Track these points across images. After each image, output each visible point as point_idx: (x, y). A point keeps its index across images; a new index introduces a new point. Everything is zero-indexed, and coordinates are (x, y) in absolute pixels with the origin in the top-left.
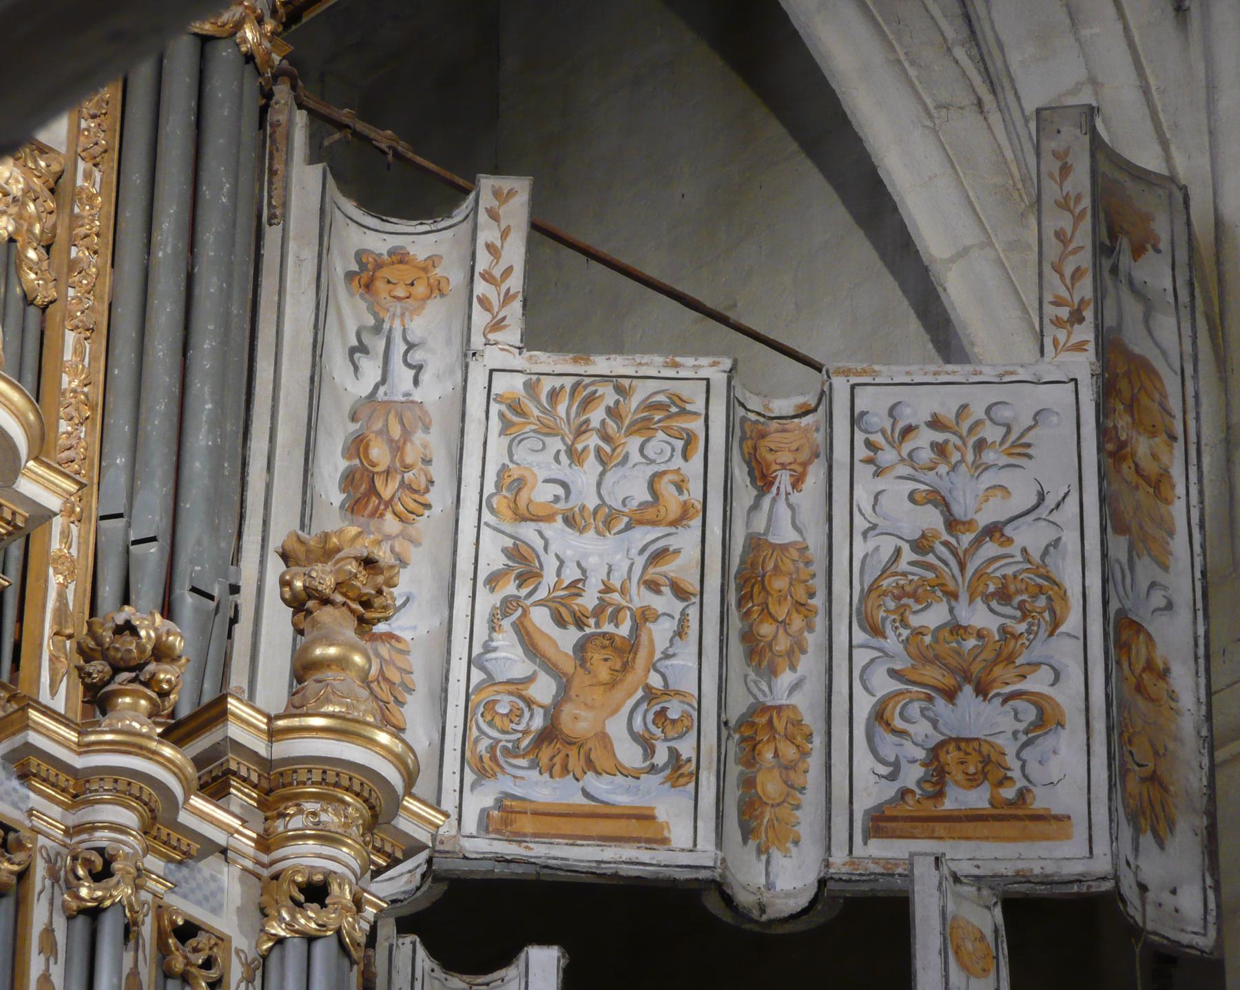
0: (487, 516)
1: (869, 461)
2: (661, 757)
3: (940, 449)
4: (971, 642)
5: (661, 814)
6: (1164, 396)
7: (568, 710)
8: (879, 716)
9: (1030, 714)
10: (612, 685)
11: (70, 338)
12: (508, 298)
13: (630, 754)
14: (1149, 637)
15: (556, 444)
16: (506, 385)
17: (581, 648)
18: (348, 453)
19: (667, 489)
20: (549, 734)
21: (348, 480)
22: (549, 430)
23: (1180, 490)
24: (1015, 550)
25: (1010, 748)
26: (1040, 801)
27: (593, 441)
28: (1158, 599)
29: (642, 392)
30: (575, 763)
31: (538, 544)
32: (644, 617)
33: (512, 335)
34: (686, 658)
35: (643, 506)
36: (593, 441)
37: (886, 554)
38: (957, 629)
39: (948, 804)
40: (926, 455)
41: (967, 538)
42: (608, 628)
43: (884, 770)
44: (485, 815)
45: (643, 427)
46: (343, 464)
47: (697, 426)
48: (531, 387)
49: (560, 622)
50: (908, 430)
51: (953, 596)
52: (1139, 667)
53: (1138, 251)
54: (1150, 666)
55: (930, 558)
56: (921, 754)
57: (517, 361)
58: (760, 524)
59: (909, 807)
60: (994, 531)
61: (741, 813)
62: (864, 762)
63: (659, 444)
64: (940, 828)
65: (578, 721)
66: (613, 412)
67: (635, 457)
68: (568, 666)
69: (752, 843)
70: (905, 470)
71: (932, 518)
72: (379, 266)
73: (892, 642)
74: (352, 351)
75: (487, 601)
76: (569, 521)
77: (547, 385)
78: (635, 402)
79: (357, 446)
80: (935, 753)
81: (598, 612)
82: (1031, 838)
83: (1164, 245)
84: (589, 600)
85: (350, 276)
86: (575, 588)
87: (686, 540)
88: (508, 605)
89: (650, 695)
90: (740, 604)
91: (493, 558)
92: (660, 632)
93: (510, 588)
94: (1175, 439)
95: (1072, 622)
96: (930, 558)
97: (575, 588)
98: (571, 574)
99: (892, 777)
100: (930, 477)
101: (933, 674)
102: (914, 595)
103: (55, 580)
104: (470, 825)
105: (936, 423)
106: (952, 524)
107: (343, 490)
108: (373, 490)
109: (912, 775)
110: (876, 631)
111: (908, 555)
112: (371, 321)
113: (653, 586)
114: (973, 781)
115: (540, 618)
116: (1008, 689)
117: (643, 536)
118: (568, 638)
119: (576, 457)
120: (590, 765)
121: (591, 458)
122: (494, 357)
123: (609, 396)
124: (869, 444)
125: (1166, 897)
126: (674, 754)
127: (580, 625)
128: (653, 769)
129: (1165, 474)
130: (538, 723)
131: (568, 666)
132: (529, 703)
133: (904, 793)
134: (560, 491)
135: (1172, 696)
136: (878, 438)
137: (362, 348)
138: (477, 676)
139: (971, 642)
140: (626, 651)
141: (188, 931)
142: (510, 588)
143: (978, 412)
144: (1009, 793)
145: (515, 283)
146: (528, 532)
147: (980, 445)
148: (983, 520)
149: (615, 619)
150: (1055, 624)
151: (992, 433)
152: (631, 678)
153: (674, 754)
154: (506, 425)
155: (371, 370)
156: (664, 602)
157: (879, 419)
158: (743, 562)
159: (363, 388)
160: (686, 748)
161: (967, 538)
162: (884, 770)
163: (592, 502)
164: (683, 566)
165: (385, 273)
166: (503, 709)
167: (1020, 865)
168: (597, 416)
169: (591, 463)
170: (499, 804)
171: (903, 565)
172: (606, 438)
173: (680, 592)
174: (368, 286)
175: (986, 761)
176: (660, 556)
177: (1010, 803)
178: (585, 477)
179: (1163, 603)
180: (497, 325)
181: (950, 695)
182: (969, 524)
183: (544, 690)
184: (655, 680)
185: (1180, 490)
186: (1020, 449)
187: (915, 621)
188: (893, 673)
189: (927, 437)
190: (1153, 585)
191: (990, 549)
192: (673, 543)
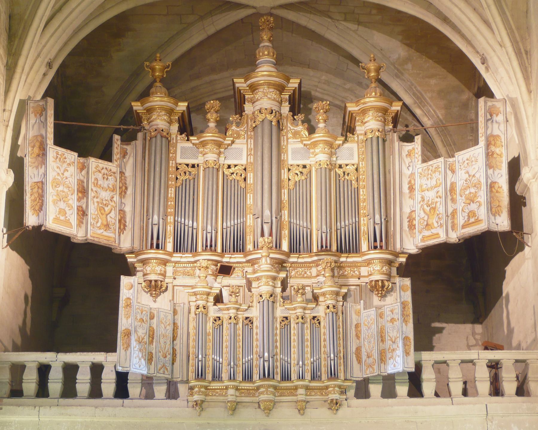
0: (419, 193)
1: (460, 168)
2: (439, 224)
3: (468, 164)
4: (472, 195)
5: (440, 233)
6: (501, 139)
7: (429, 220)
8: (462, 210)
9: (478, 204)
10: (433, 215)
11: (361, 190)
12: (419, 156)
13: (436, 225)
14: (498, 183)
15: (426, 178)
16: (420, 170)
17: (430, 210)
18: (408, 184)
19: (438, 181)
20: (427, 225)
21: (409, 188)
22: (425, 176)
23: (504, 155)
24: (476, 178)
25: (476, 210)
26: (480, 218)
27: (429, 176)
28: (499, 176)
29: (435, 166)
30: (430, 228)
31: (424, 195)
32: (436, 203)
33: (420, 162)
34: (441, 208)
35: (436, 184)
36: (429, 176)
37: (462, 183)
38: (470, 193)
39: (470, 222)
40: (466, 165)
41: (471, 178)
42: (432, 206)
43: (463, 218)
44: (421, 239)
45: (435, 172)
46: (408, 186)
47: (440, 169)
48: (422, 170)
49: (427, 207)
50: (464, 161)
51: (470, 188)
52: (497, 187)
53: (497, 115)
54: (499, 187)
55: (467, 182)
56: (467, 214)
57: (420, 166)
58: (453, 180)
59: (466, 224)
60: (474, 176)
61: (452, 227)
62: (461, 218)
63: (437, 173)
64: (469, 225)
65: (430, 222)
66: (432, 171)
67: (434, 177)
68: (428, 213)
69: (454, 231)
70: (464, 169)
71: (467, 175)
72: (411, 151)
73: (463, 198)
74: (408, 167)
75: (419, 206)
76: (427, 190)
77: (424, 168)
78: (434, 168)
79: (410, 182)
80: (468, 214)
81: (431, 204)
82: (479, 224)
83: (502, 112)
84: (430, 202)
85: (407, 155)
86: (429, 201)
87: (440, 189)
88: (422, 205)
89: (438, 215)
90: (450, 194)
91: (420, 199)
92: (438, 204)
93: (422, 203)
94: (503, 146)
95: (482, 189)
96: (467, 182)
97: (429, 201)
98: (428, 198)
99: (464, 219)
100: (467, 169)
101: (468, 201)
102: (465, 189)
103: (362, 228)
104: (419, 241)
105: (467, 160)
106: (469, 176)
107: (408, 189)
108: (413, 188)
109: (466, 217)
110: (461, 196)
111: (465, 183)
112: (410, 161)
113: (437, 197)
114: (472, 217)
115: (425, 206)
116: (476, 201)
117: (436, 189)
118: (428, 209)
119: (428, 179)
120: (432, 228)
121: (429, 179)
122: (418, 166)
123: (431, 167)
124: (460, 166)
125: (502, 224)
126: (441, 223)
127: (429, 206)
128: (438, 226)
129: (502, 153)
130: (426, 223)
131: (428, 213)
132: (424, 220)
133: (466, 221)
134: (426, 185)
135: (503, 190)
136: (461, 164)
137: (409, 166)
138: (419, 218)
139: (472, 195)
140: (434, 209)
141: (314, 318)
142: (422, 203)
143: (472, 156)
144: (476, 218)
145: (420, 153)
146: (423, 193)
147: (472, 161)
148: (473, 174)
149: (433, 204)
150: (481, 189)
151: (473, 159)
152: (435, 213)
153: (441, 223)
154: (420, 177)
155: (411, 168)
156: (439, 200)
157: (461, 161)
158: (450, 187)
159: (410, 172)
160: (442, 222)
161: (471, 178)
162: (463, 218)
163: (430, 186)
164: (440, 194)
165: (412, 152)
166: (422, 222)
167: (478, 229)
168: (430, 172)
169: (430, 180)
170: (422, 237)
171: (464, 184)
172: (431, 175)
173: (440, 197)
174: (410, 155)
175: (474, 213)
176: (438, 192)
177: (477, 219)
178: (428, 182)
179: (500, 176)
180: (418, 161)
181: (470, 204)
182: (471, 175)
183: (426, 218)
184: (438, 212)
185: (504, 155)
186: (476, 161)
187: (466, 193)
188: (464, 203)
189: (467, 162)
190: (498, 174)
191: (474, 179)
192: (439, 190)
